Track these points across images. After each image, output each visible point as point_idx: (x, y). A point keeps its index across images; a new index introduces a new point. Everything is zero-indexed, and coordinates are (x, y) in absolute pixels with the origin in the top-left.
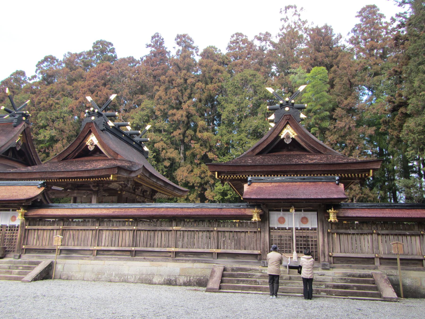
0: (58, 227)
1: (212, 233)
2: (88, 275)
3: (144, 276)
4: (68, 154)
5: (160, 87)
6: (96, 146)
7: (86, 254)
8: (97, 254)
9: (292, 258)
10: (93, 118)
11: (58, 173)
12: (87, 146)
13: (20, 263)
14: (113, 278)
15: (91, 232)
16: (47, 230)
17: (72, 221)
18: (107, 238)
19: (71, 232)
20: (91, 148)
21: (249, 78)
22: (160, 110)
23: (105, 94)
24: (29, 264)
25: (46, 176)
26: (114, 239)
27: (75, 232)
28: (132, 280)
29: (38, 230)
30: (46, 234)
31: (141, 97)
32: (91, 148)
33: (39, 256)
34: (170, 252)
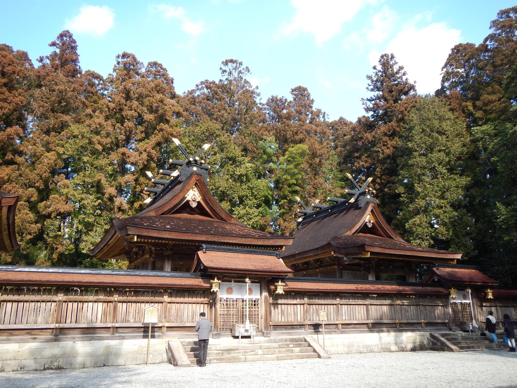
0: (302, 301)
1: (418, 307)
2: (341, 349)
3: (384, 345)
4: (169, 208)
5: (94, 111)
6: (199, 203)
7: (331, 329)
8: (342, 328)
9: (472, 324)
10: (195, 169)
11: (230, 238)
12: (188, 201)
13: (281, 340)
14: (361, 349)
15: (332, 306)
16: (291, 304)
17: (410, 297)
18: (346, 312)
19: (314, 306)
20: (194, 205)
21: (217, 132)
22: (99, 143)
23: (20, 102)
24: (290, 342)
25: (214, 240)
26: (352, 314)
27: (317, 306)
28: (376, 350)
29: (281, 304)
30: (291, 308)
31: (66, 118)
32: (194, 205)
33: (289, 333)
34: (395, 324)
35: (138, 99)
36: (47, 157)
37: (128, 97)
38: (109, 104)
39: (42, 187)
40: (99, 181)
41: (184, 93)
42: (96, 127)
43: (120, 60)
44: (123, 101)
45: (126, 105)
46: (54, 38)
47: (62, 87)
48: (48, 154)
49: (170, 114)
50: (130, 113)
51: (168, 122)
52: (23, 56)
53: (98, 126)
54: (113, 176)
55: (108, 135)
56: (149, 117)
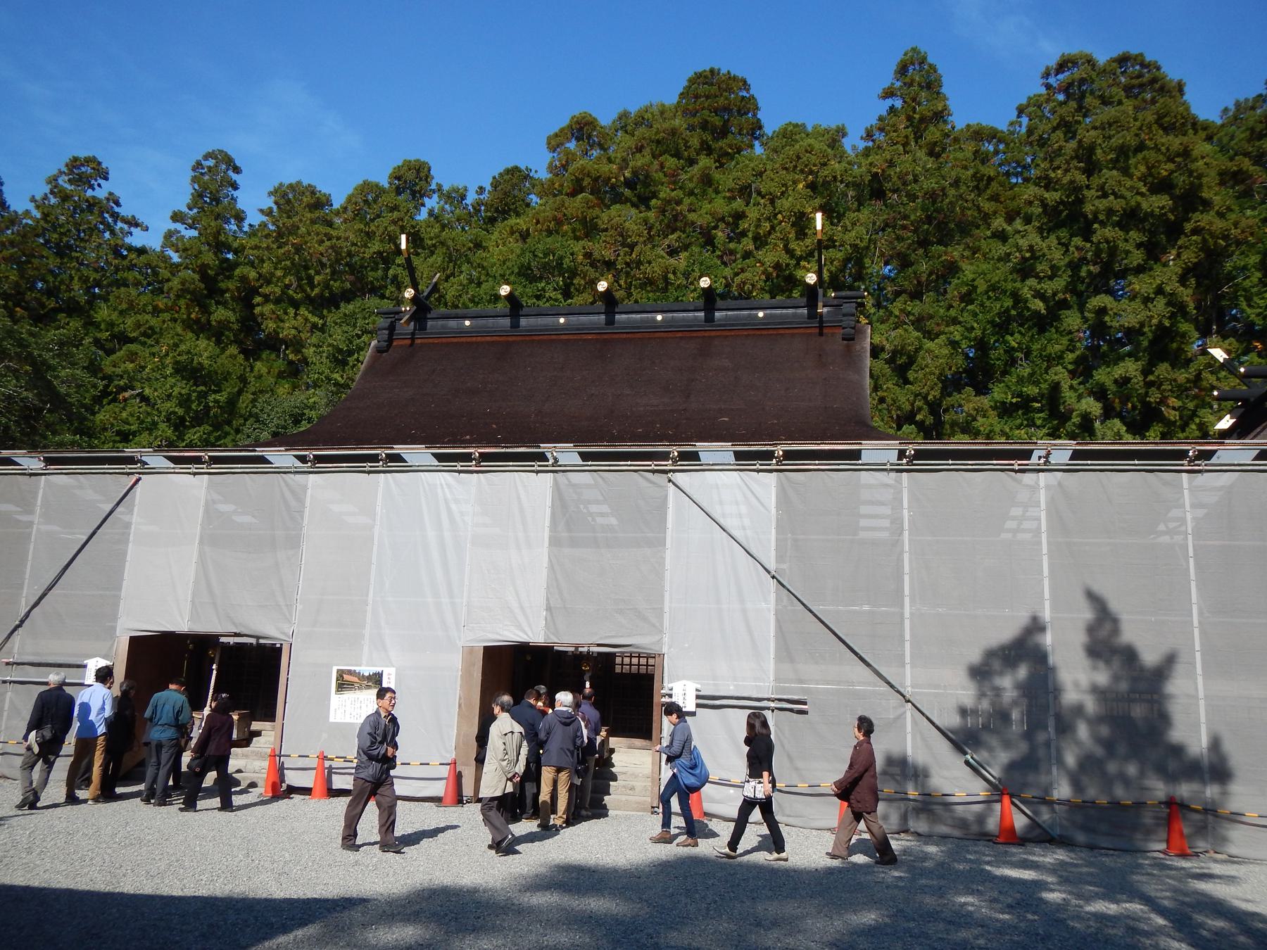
22: (1040, 295)
31: (955, 252)
35: (1114, 164)
36: (929, 351)
37: (1091, 169)
38: (1047, 195)
39: (930, 420)
40: (1056, 387)
41: (1226, 110)
42: (1023, 258)
43: (1052, 80)
44: (1081, 179)
45: (1088, 187)
46: (887, 78)
47: (930, 184)
48: (929, 345)
49: (1211, 178)
50: (1102, 204)
51: (1207, 204)
52: (835, 138)
53: (1028, 255)
54: (1083, 369)
55: (1054, 272)
56: (1159, 203)
